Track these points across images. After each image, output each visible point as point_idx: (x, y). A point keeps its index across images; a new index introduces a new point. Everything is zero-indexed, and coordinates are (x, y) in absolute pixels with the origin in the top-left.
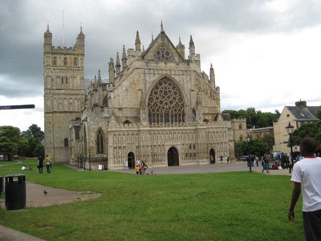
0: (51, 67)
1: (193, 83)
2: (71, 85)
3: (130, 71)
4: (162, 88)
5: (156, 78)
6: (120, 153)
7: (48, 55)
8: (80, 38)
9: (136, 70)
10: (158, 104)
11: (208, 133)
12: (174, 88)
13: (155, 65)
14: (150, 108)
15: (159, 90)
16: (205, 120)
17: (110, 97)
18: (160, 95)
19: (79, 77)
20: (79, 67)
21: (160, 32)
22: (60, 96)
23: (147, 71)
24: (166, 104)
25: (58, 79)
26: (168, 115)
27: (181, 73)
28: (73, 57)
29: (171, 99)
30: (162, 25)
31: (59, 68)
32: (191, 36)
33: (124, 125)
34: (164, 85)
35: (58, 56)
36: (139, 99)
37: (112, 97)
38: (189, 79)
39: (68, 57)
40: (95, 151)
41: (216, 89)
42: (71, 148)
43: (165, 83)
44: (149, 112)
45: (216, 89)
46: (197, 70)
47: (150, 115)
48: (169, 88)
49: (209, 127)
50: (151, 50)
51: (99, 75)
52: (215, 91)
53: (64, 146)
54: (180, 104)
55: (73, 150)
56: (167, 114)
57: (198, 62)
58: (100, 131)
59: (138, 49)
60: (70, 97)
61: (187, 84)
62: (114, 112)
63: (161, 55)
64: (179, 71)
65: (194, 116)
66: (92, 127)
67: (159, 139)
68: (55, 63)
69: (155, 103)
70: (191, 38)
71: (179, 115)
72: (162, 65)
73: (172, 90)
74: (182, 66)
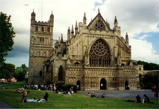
0: (34, 32)
1: (116, 42)
2: (45, 42)
3: (80, 34)
4: (98, 45)
5: (94, 39)
6: (72, 81)
7: (33, 25)
8: (51, 17)
9: (83, 34)
10: (95, 54)
11: (124, 72)
12: (104, 45)
13: (94, 32)
14: (90, 56)
16: (123, 65)
17: (68, 49)
18: (97, 49)
19: (49, 39)
20: (50, 33)
21: (98, 14)
22: (39, 48)
23: (89, 35)
24: (100, 54)
25: (38, 38)
28: (47, 27)
29: (103, 52)
30: (99, 10)
31: (39, 33)
32: (116, 17)
33: (75, 65)
35: (39, 26)
36: (85, 50)
37: (69, 49)
38: (114, 41)
39: (44, 27)
40: (57, 79)
41: (129, 47)
42: (43, 77)
43: (100, 42)
44: (90, 58)
45: (129, 47)
46: (118, 36)
48: (102, 45)
49: (125, 68)
50: (92, 23)
51: (62, 36)
53: (39, 76)
54: (108, 54)
55: (44, 78)
56: (100, 60)
57: (119, 31)
58: (61, 68)
59: (85, 23)
60: (44, 48)
61: (112, 43)
62: (70, 57)
63: (98, 27)
64: (108, 36)
65: (116, 62)
66: (56, 65)
67: (95, 73)
68: (37, 30)
69: (94, 53)
70: (116, 18)
71: (107, 61)
72: (98, 32)
73: (104, 47)
74: (110, 33)
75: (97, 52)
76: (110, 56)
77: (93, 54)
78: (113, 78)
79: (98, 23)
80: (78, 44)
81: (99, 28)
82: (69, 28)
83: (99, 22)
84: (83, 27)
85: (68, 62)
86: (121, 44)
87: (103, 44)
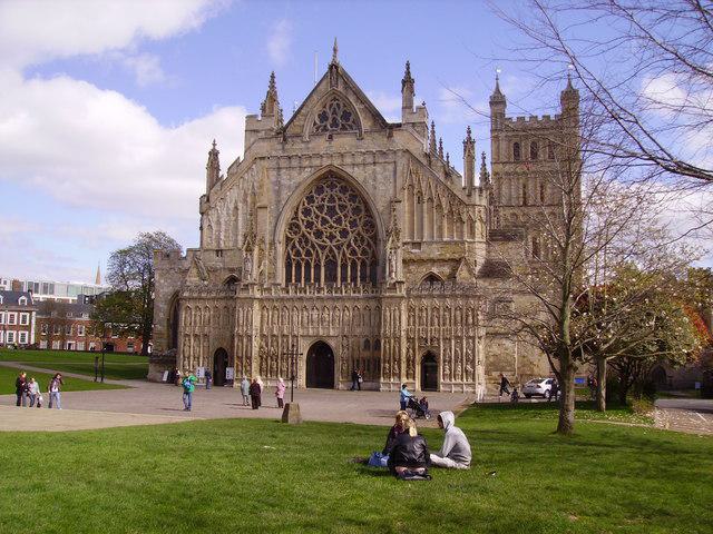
12: (353, 198)
14: (289, 248)
15: (316, 204)
16: (432, 278)
18: (317, 217)
23: (283, 163)
26: (336, 263)
27: (370, 160)
34: (328, 192)
41: (469, 195)
43: (332, 187)
44: (288, 257)
46: (412, 149)
47: (288, 266)
48: (340, 199)
52: (465, 199)
56: (331, 264)
70: (408, 69)
72: (321, 144)
73: (348, 204)
74: (374, 143)
75: (318, 230)
76: (375, 243)
77: (300, 242)
78: (362, 340)
79: (331, 105)
80: (240, 205)
81: (337, 126)
82: (214, 145)
83: (335, 99)
84: (259, 135)
85: (192, 279)
86: (423, 185)
87: (347, 195)
